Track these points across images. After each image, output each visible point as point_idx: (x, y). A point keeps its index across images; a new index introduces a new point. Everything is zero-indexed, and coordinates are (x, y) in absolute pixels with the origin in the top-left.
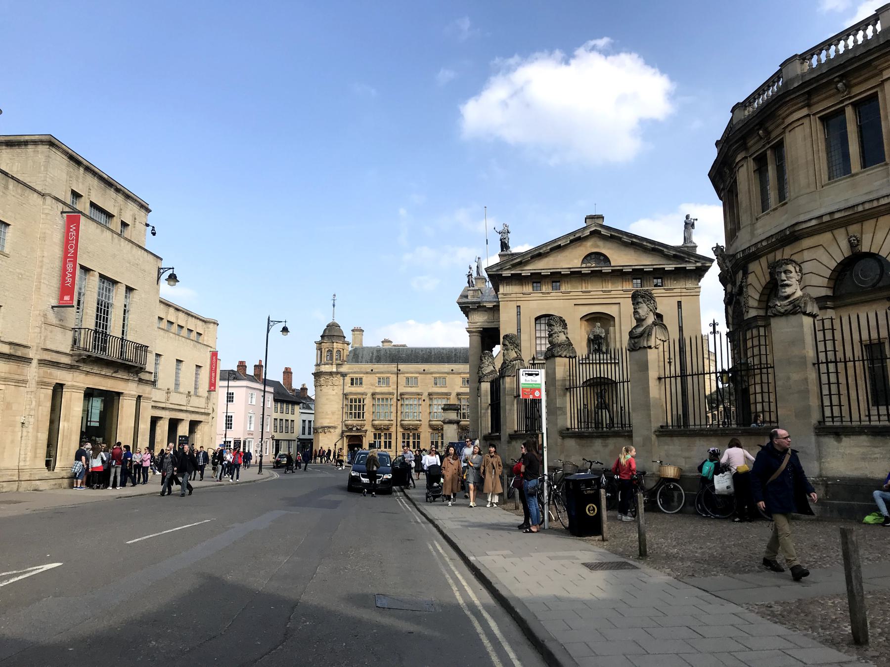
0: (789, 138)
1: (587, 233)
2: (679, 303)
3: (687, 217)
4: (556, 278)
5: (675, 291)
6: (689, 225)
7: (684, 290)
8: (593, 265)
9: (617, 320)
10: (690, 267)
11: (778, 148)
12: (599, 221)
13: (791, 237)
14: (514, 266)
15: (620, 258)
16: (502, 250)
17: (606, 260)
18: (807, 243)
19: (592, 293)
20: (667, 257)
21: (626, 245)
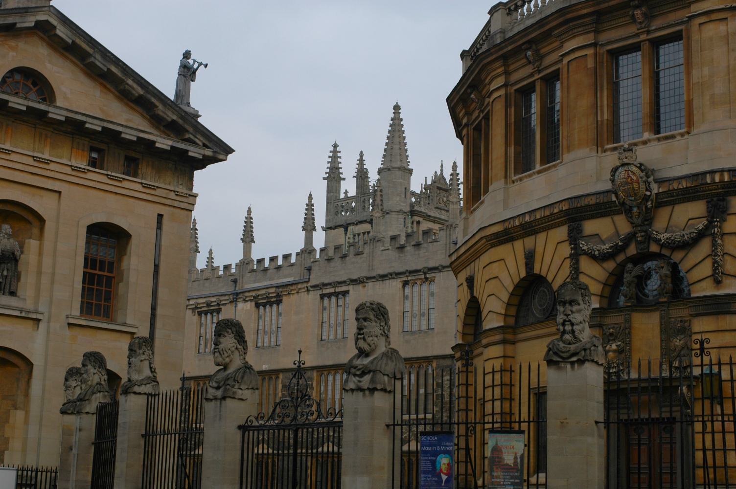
1: (29, 21)
2: (160, 216)
3: (187, 55)
5: (158, 192)
6: (187, 72)
7: (172, 195)
9: (48, 225)
10: (195, 152)
19: (13, 157)
20: (157, 121)
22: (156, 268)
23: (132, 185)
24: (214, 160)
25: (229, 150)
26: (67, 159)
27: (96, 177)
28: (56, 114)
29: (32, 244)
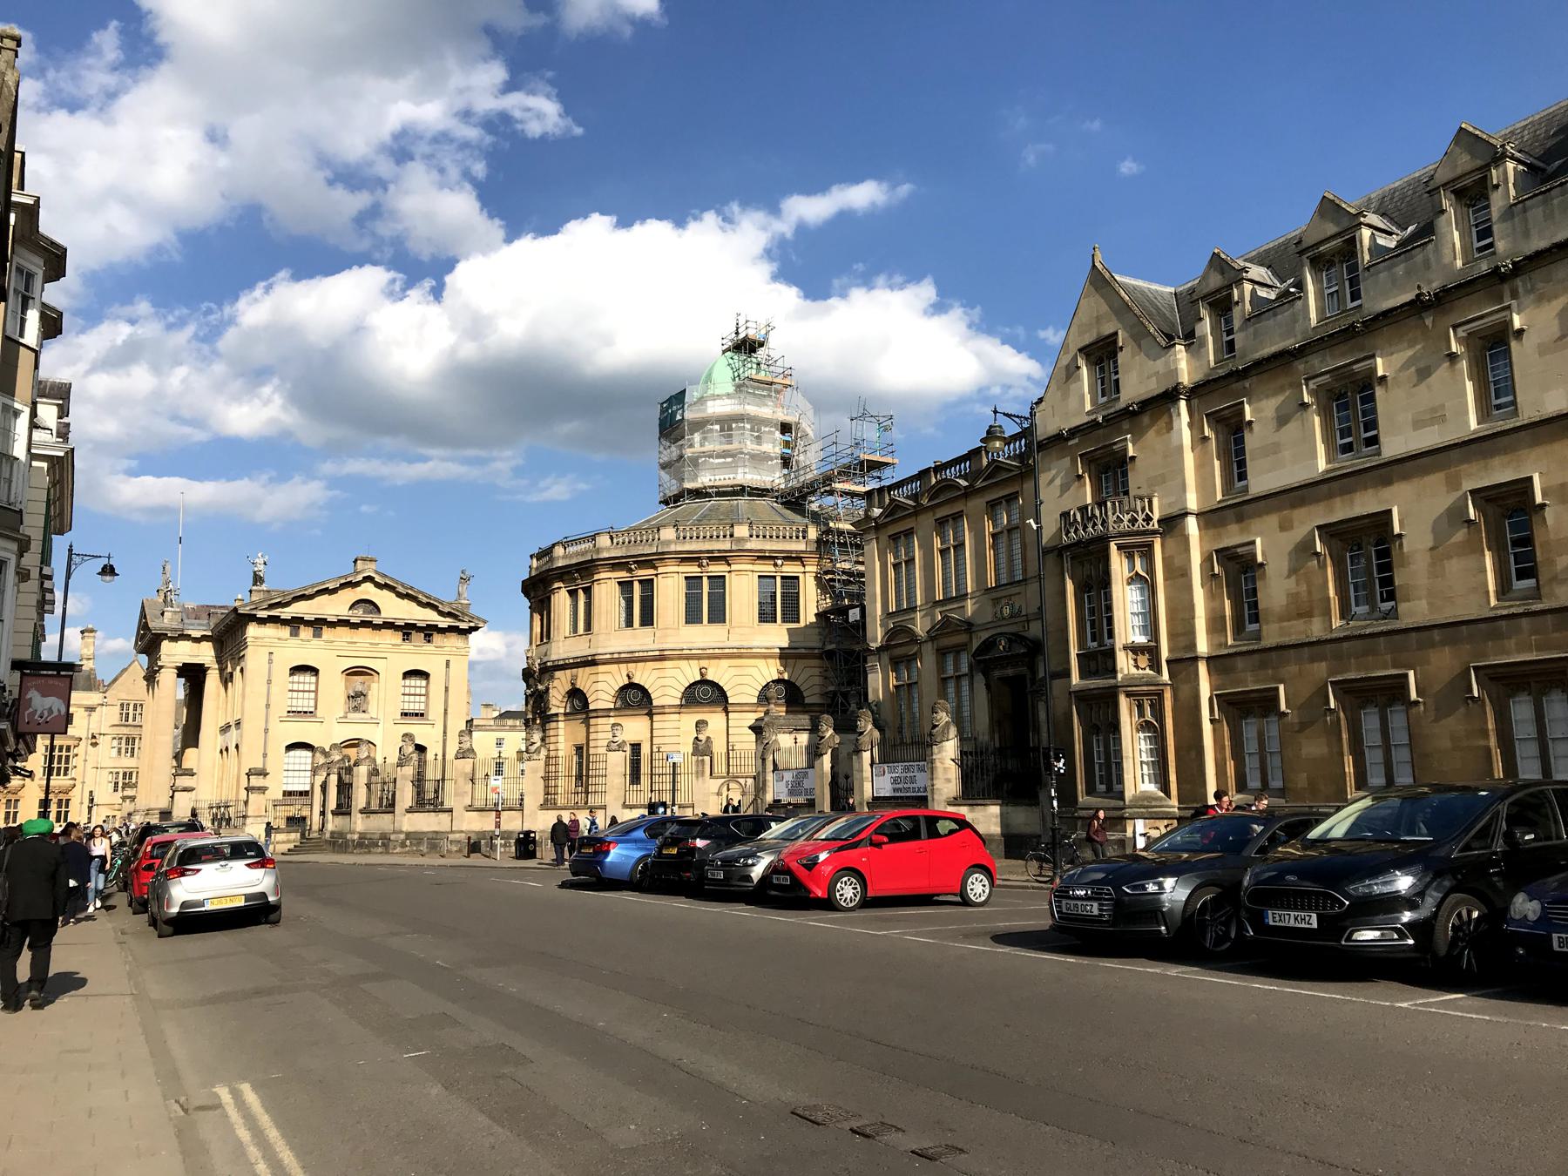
0: (596, 588)
1: (360, 578)
4: (319, 624)
8: (358, 615)
10: (463, 626)
11: (588, 591)
12: (373, 566)
13: (590, 662)
14: (271, 607)
15: (394, 608)
16: (255, 584)
17: (374, 607)
18: (601, 668)
20: (441, 613)
21: (400, 595)
22: (447, 689)
23: (429, 647)
24: (476, 629)
25: (485, 622)
26: (391, 638)
27: (407, 646)
28: (378, 621)
29: (374, 686)
